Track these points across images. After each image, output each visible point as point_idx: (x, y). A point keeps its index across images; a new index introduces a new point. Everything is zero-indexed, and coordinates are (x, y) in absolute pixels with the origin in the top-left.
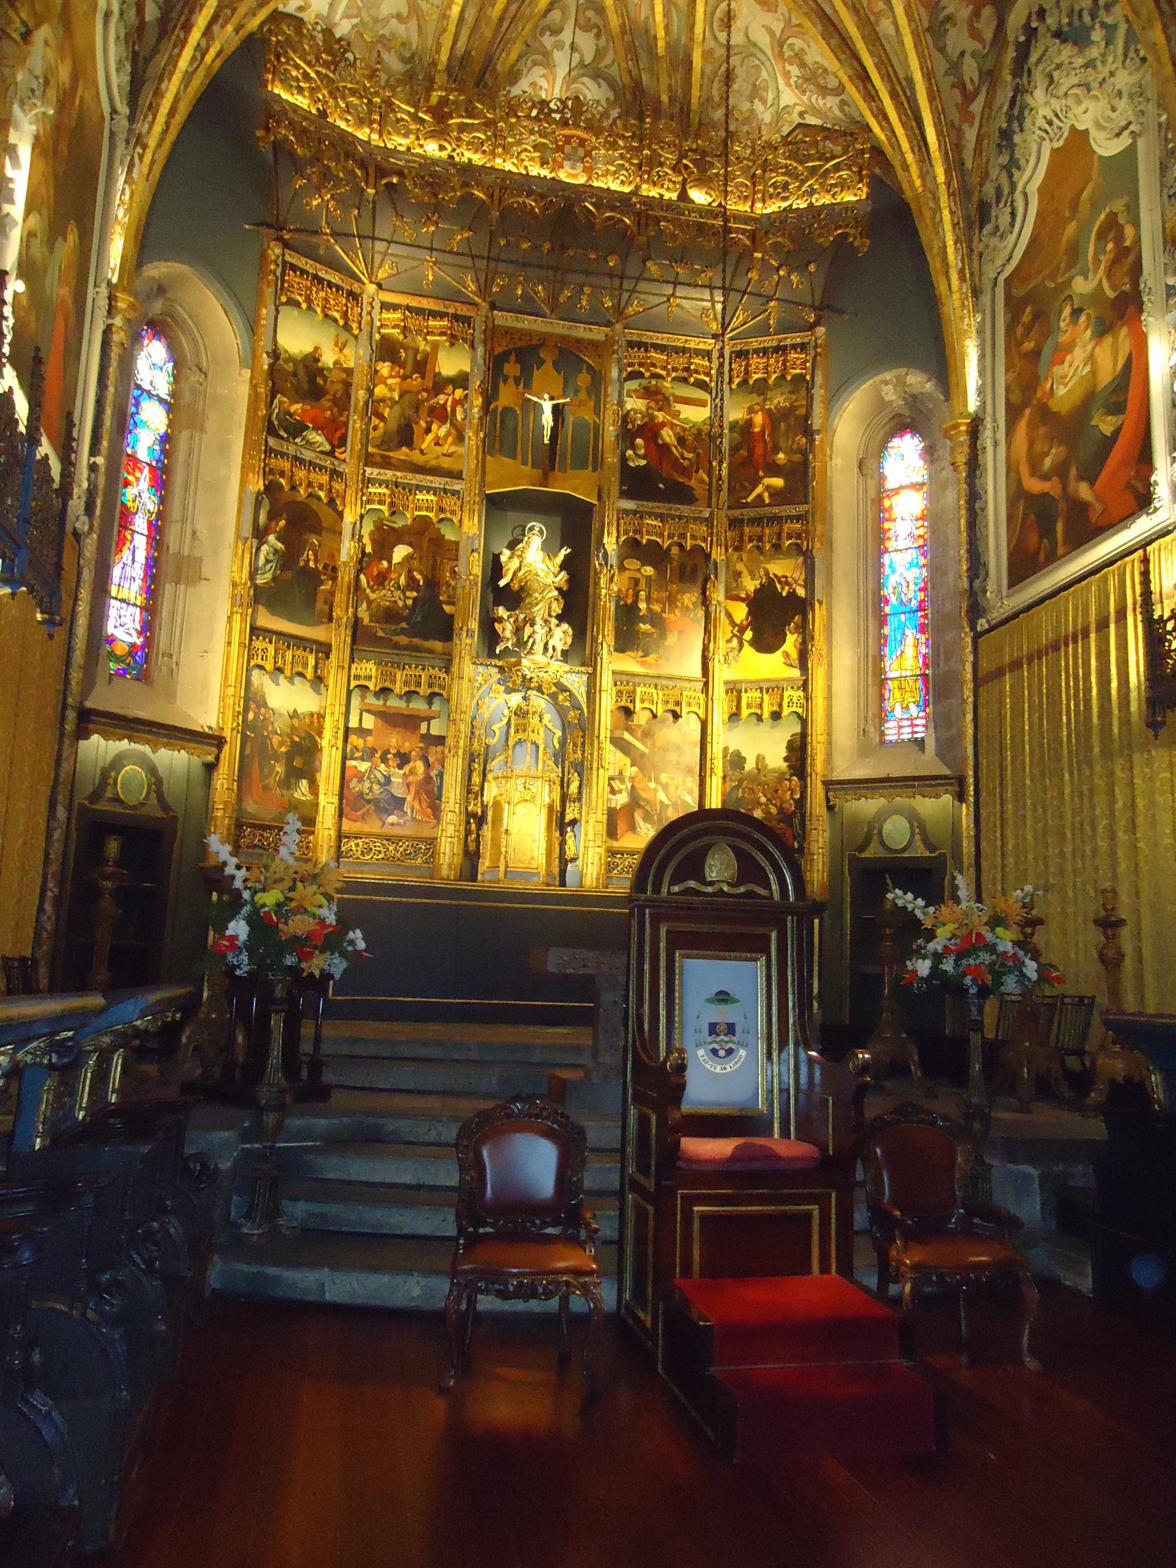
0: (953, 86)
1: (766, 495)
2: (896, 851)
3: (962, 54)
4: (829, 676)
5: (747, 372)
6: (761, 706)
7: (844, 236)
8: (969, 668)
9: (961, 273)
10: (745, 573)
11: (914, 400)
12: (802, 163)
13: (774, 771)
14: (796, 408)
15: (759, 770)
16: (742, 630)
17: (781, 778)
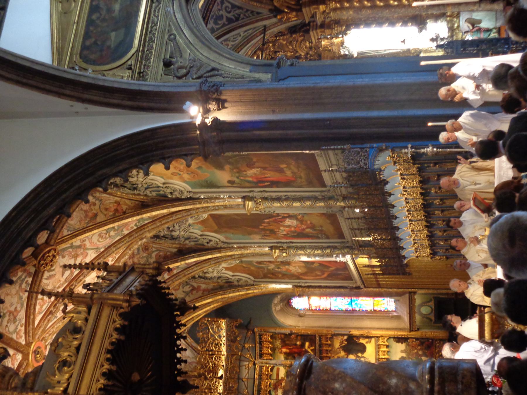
0: (192, 294)
1: (311, 348)
2: (432, 311)
3: (183, 292)
4: (374, 329)
5: (268, 354)
6: (384, 351)
7: (236, 327)
8: (375, 290)
9: (248, 289)
10: (339, 355)
11: (282, 300)
12: (209, 339)
13: (406, 348)
14: (281, 337)
15: (405, 352)
16: (358, 357)
17: (408, 345)
